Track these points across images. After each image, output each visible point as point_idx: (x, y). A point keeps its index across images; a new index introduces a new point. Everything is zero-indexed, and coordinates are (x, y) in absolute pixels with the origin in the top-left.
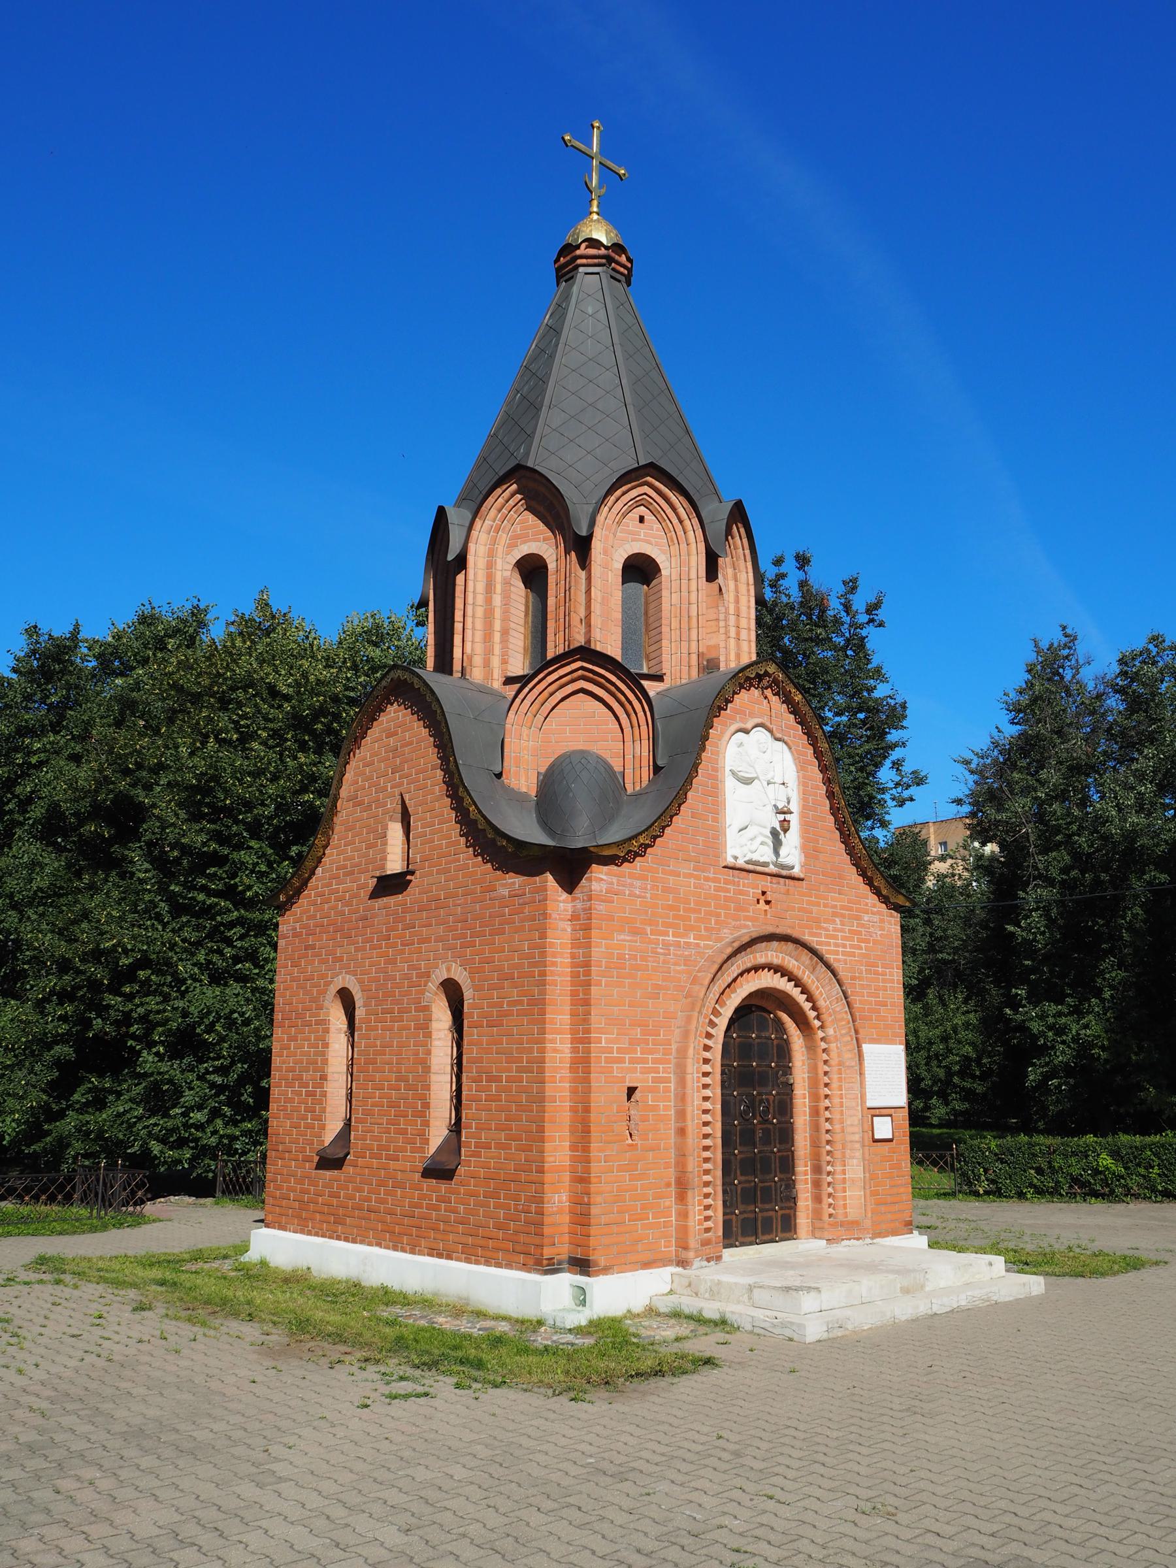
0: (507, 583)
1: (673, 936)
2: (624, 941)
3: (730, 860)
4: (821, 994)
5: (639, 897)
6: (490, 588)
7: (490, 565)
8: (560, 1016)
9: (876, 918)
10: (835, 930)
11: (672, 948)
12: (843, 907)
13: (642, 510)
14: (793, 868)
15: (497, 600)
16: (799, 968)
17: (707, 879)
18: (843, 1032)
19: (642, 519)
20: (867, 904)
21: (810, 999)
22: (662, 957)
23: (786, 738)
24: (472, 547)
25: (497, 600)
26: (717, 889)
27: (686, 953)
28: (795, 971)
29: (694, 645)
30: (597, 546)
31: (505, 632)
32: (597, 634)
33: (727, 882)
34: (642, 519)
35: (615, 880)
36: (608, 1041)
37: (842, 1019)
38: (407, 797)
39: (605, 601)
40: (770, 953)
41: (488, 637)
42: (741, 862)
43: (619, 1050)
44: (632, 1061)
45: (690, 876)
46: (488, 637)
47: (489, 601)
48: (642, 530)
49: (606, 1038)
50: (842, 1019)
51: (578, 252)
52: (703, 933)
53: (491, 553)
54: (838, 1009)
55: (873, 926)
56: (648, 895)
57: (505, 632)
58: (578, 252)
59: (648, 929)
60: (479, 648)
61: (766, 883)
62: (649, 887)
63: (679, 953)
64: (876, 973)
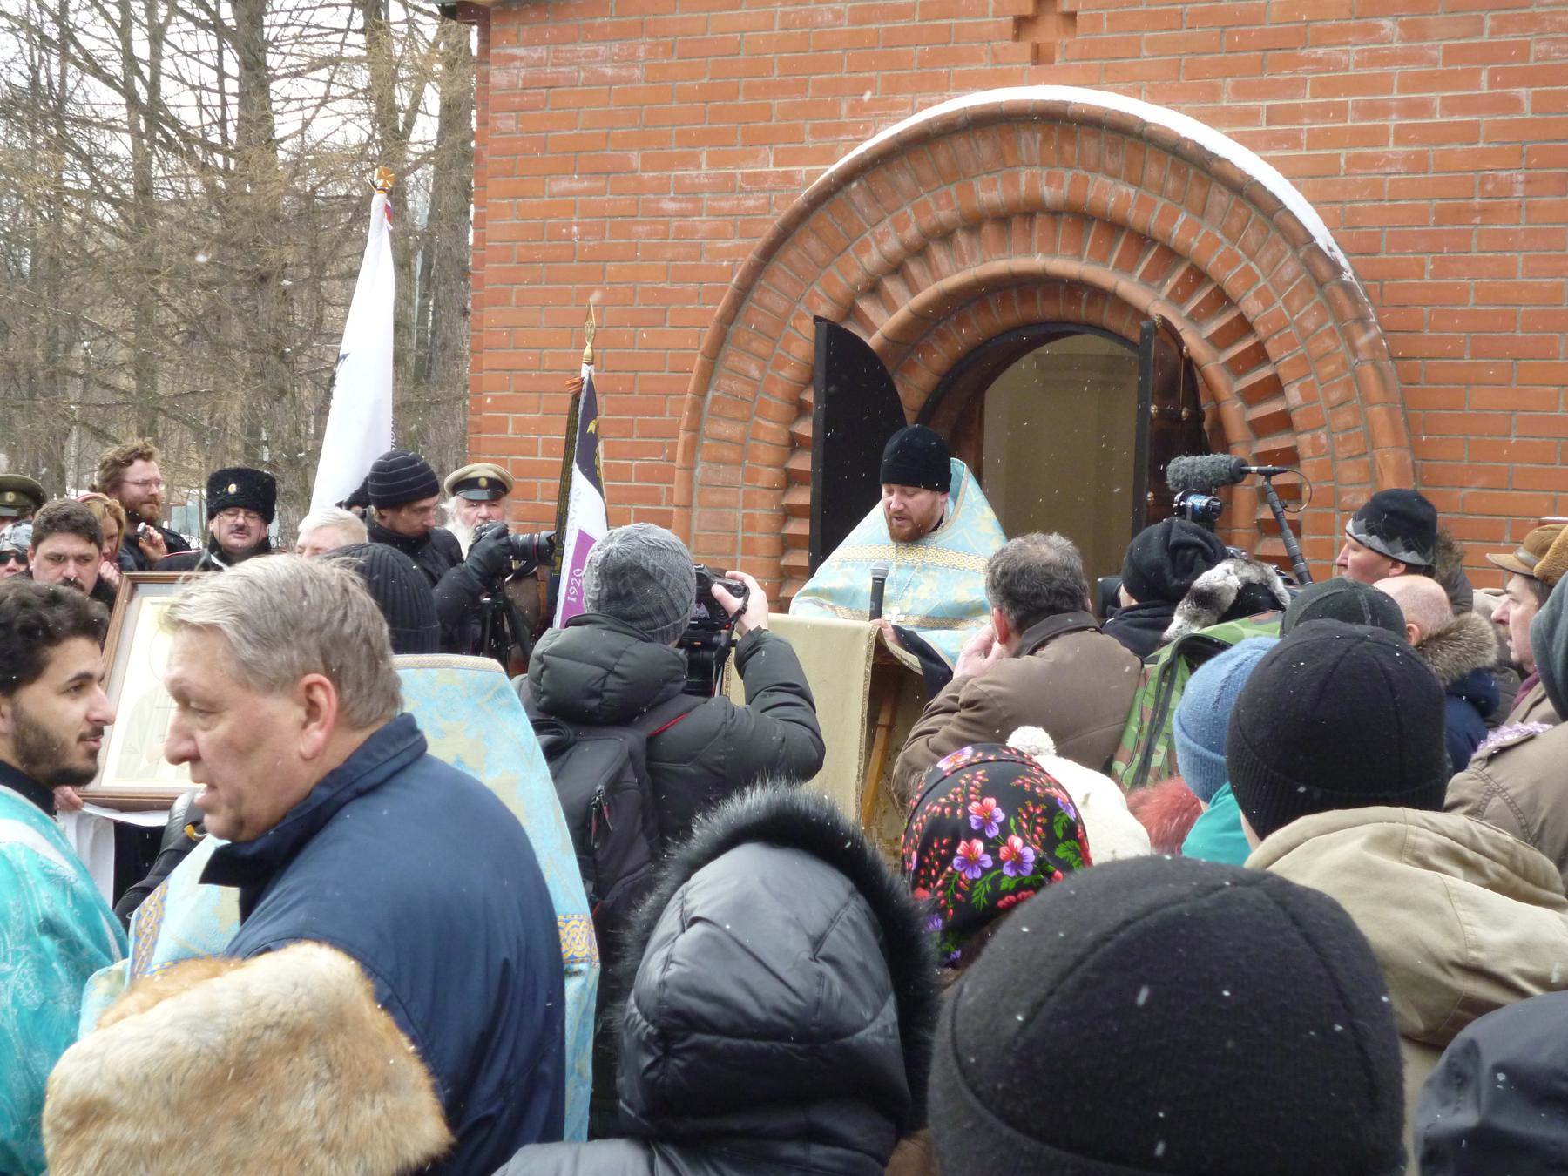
1: (711, 164)
4: (1249, 277)
11: (707, 195)
18: (1335, 396)
22: (675, 222)
27: (750, 203)
28: (1132, 215)
36: (522, 426)
37: (1326, 356)
49: (517, 421)
52: (810, 142)
54: (1309, 324)
56: (637, 72)
62: (641, 52)
63: (726, 205)
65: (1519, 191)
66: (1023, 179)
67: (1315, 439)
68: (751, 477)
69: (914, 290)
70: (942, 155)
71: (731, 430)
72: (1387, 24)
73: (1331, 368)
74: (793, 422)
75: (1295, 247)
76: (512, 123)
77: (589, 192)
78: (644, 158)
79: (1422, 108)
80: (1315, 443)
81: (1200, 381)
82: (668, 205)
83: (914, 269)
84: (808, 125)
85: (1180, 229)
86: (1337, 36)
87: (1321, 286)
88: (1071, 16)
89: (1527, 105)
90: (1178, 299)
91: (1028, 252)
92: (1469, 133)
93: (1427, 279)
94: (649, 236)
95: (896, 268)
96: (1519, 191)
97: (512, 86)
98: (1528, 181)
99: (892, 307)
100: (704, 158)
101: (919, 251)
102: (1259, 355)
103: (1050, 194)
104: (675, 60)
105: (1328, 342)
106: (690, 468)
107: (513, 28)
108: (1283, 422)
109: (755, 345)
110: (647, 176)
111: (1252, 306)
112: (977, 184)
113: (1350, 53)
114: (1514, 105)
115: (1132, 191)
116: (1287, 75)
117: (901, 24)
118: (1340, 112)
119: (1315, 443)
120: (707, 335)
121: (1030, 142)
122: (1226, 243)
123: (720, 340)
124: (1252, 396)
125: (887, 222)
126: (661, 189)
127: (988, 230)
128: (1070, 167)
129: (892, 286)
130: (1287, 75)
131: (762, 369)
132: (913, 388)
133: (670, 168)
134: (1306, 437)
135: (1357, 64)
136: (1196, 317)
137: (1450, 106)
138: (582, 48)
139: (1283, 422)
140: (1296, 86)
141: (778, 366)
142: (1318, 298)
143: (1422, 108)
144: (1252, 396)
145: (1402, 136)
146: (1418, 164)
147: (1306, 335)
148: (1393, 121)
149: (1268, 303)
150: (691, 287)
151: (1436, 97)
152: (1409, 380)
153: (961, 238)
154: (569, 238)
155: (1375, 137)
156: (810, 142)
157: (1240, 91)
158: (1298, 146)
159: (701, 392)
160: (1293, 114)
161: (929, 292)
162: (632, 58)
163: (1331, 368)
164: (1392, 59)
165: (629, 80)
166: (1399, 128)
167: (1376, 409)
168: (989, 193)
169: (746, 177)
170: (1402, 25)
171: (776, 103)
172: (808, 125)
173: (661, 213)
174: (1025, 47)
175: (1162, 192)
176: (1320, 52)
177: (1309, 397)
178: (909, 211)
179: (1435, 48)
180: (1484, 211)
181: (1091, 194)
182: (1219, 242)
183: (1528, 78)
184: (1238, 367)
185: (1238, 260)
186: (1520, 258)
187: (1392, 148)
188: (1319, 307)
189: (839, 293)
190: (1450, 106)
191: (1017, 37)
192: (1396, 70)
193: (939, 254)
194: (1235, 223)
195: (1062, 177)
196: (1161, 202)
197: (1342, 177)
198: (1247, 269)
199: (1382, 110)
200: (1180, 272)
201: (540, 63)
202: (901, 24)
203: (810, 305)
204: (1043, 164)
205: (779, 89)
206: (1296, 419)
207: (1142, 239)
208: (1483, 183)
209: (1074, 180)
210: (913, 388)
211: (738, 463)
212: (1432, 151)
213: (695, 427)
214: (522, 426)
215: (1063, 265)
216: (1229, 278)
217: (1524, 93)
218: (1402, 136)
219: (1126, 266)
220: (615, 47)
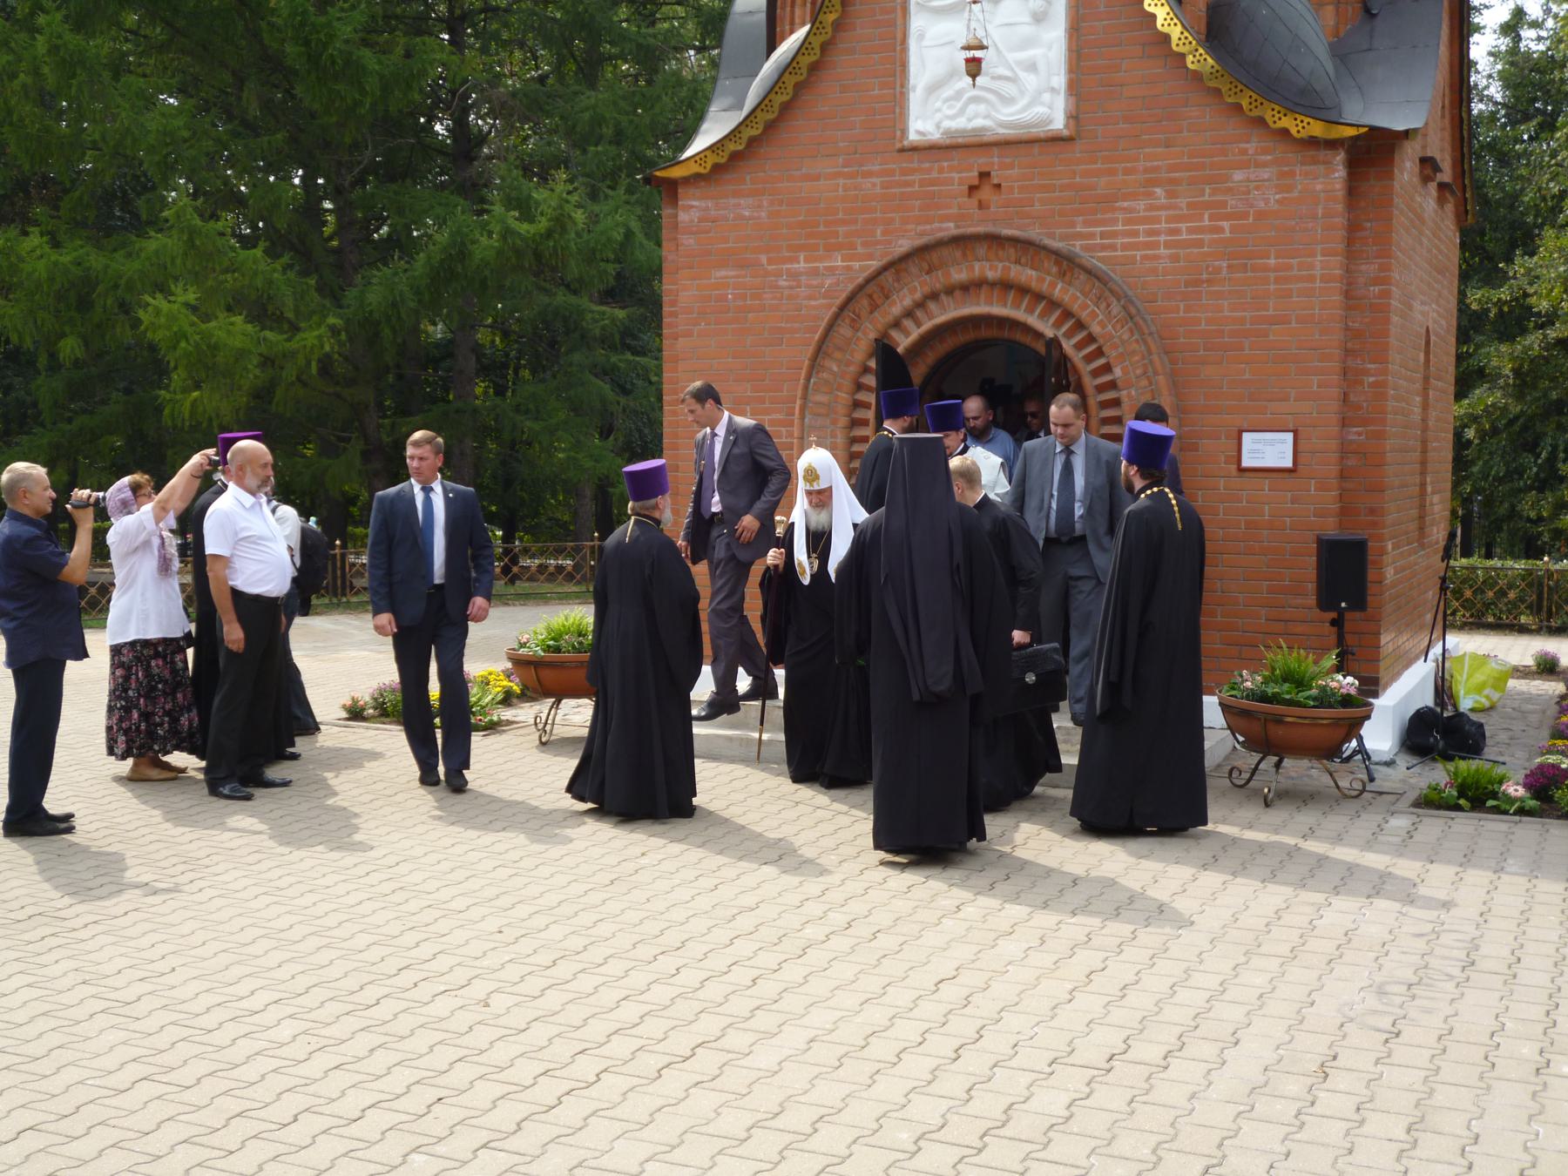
1: (806, 260)
3: (913, 136)
4: (1094, 315)
5: (750, 218)
9: (1265, 174)
10: (1151, 208)
12: (1172, 169)
17: (869, 174)
18: (1138, 372)
20: (1244, 152)
26: (885, 186)
28: (1034, 285)
33: (904, 172)
37: (1134, 352)
40: (977, 266)
42: (935, 136)
52: (860, 250)
54: (1125, 337)
55: (1257, 188)
56: (763, 214)
59: (764, 259)
61: (980, 161)
62: (765, 203)
63: (815, 282)
64: (1266, 269)
65: (1224, 271)
66: (977, 269)
67: (1129, 393)
68: (834, 422)
69: (919, 324)
70: (935, 256)
71: (819, 398)
72: (1158, 191)
73: (1136, 358)
74: (854, 394)
75: (1119, 300)
76: (692, 241)
77: (737, 277)
79: (1176, 232)
81: (1069, 365)
82: (783, 283)
83: (919, 314)
85: (1058, 291)
86: (1133, 196)
87: (1132, 318)
88: (998, 186)
89: (1227, 230)
90: (1057, 325)
91: (978, 304)
92: (1200, 243)
93: (1181, 314)
94: (772, 299)
95: (909, 314)
96: (1224, 271)
97: (692, 221)
98: (1229, 267)
99: (907, 333)
100: (802, 258)
101: (920, 305)
102: (1099, 353)
103: (991, 275)
104: (784, 207)
105: (1135, 346)
106: (802, 418)
107: (691, 191)
108: (1112, 385)
109: (838, 355)
110: (770, 268)
111: (1096, 329)
112: (952, 270)
113: (1141, 205)
114: (1221, 230)
115: (1034, 273)
117: (909, 189)
118: (1135, 234)
119: (1129, 395)
120: (811, 349)
121: (981, 250)
122: (1082, 298)
123: (819, 350)
124: (1096, 373)
125: (905, 290)
126: (779, 274)
127: (958, 293)
128: (1001, 261)
129: (908, 323)
131: (839, 366)
132: (918, 373)
133: (784, 263)
134: (1124, 393)
135: (1145, 210)
136: (1069, 335)
137: (1191, 231)
138: (732, 201)
139: (1112, 385)
140: (1115, 221)
141: (848, 364)
142: (1130, 324)
143: (1176, 232)
144: (1096, 373)
145: (1167, 245)
146: (1175, 258)
147: (1123, 342)
148: (1162, 238)
149: (1103, 327)
150: (796, 325)
151: (1183, 226)
152: (1173, 362)
153: (943, 297)
154: (726, 300)
155: (1155, 245)
156: (860, 250)
157: (1087, 224)
158: (1116, 250)
159: (808, 378)
160: (1114, 235)
161: (927, 325)
163: (1136, 358)
165: (759, 218)
166: (1165, 242)
167: (1161, 377)
168: (959, 275)
169: (825, 268)
170: (1166, 191)
171: (841, 230)
172: (859, 241)
173: (778, 287)
174: (974, 201)
175: (1049, 274)
176: (1126, 204)
177: (1124, 370)
178: (916, 284)
179: (1182, 202)
180: (1209, 281)
181: (1012, 274)
182: (1078, 298)
183: (1227, 217)
184: (1089, 359)
185: (1088, 306)
186: (1226, 303)
187: (1162, 251)
188: (1131, 331)
189: (880, 326)
190: (1191, 231)
191: (970, 196)
192: (1163, 213)
193: (932, 306)
194: (1087, 288)
195: (997, 268)
196: (1049, 278)
197: (1138, 265)
198: (1093, 311)
199: (1157, 233)
200: (1057, 313)
201: (707, 208)
202: (909, 189)
203: (865, 333)
204: (987, 260)
205: (844, 222)
206: (1119, 383)
207: (1038, 297)
208: (1207, 267)
209: (1004, 267)
210: (918, 373)
211: (827, 415)
212: (1181, 251)
213: (805, 397)
215: (997, 310)
216: (1084, 315)
217: (1226, 224)
218: (1167, 245)
219: (1030, 310)
220: (750, 201)
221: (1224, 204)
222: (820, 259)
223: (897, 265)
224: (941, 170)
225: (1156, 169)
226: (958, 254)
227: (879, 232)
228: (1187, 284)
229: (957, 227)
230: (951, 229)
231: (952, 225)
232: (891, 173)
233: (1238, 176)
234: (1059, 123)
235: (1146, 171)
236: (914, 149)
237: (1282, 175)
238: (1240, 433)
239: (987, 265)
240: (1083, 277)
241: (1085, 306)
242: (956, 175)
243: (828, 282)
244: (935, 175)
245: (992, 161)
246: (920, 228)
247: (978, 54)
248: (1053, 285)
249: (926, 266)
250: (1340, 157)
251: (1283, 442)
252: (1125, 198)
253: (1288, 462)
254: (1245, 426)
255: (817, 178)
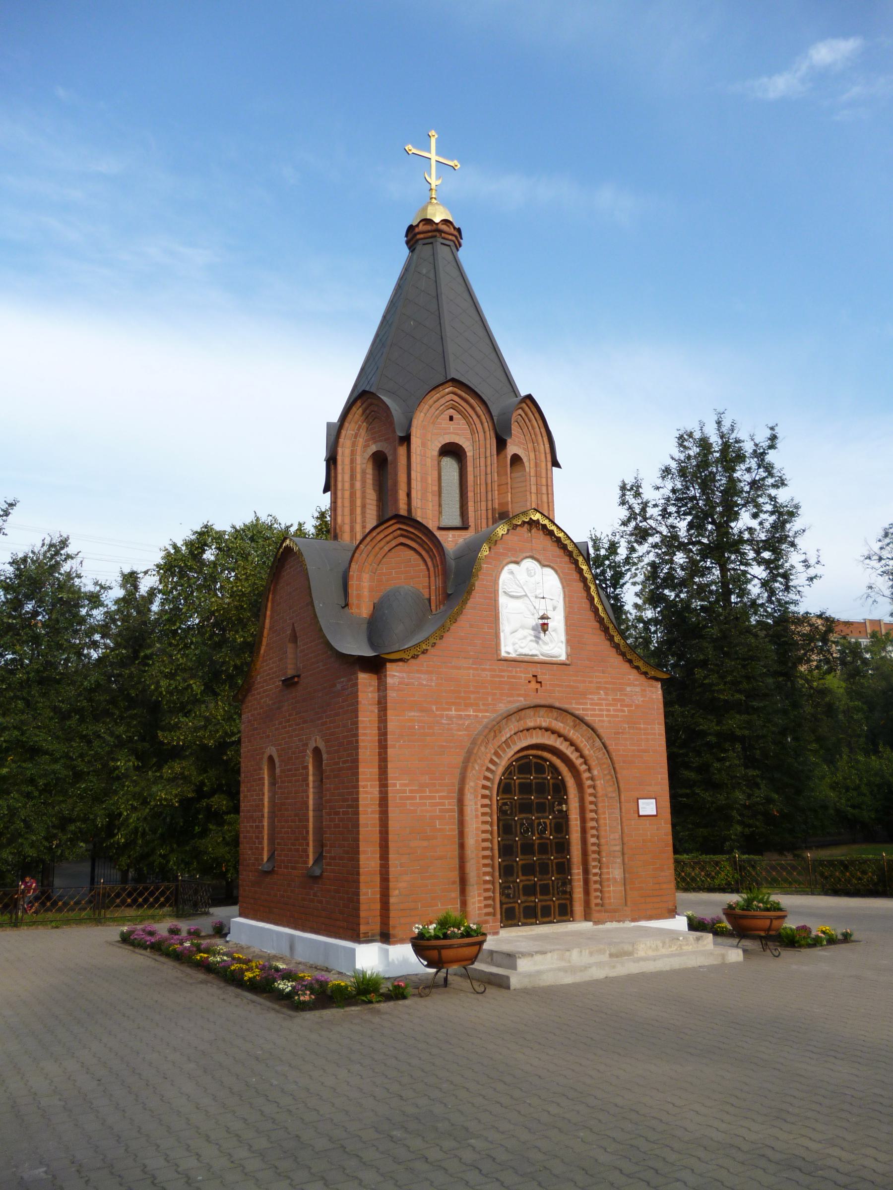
0: (364, 472)
1: (456, 710)
2: (414, 716)
3: (503, 654)
5: (426, 685)
6: (353, 478)
7: (352, 461)
8: (368, 772)
9: (638, 689)
10: (600, 699)
12: (606, 683)
13: (451, 412)
14: (560, 656)
15: (358, 485)
16: (564, 728)
17: (484, 670)
19: (451, 418)
20: (629, 679)
21: (577, 749)
23: (552, 564)
24: (340, 450)
25: (358, 485)
26: (493, 676)
28: (562, 731)
29: (490, 503)
30: (415, 441)
31: (364, 506)
32: (416, 502)
34: (451, 418)
35: (405, 675)
36: (401, 785)
37: (604, 764)
38: (296, 625)
39: (424, 479)
40: (538, 719)
41: (352, 511)
42: (513, 655)
43: (411, 791)
44: (421, 798)
45: (470, 668)
46: (352, 511)
47: (352, 486)
48: (452, 426)
49: (400, 784)
50: (604, 764)
51: (417, 230)
52: (482, 707)
53: (353, 453)
55: (635, 695)
56: (433, 684)
57: (364, 506)
58: (417, 230)
60: (347, 520)
61: (533, 670)
62: (434, 678)
63: (460, 722)
64: (640, 729)
73: (605, 766)
78: (437, 708)
80: (601, 783)
84: (481, 703)
85: (572, 734)
92: (617, 716)
103: (544, 725)
113: (596, 697)
114: (623, 711)
116: (584, 701)
119: (601, 783)
121: (542, 711)
126: (442, 716)
128: (548, 718)
130: (584, 701)
138: (417, 675)
140: (586, 704)
145: (607, 716)
146: (609, 722)
148: (605, 713)
151: (611, 708)
154: (415, 729)
157: (577, 703)
162: (431, 680)
164: (603, 699)
165: (430, 686)
168: (531, 724)
171: (472, 696)
173: (442, 724)
176: (590, 696)
177: (598, 771)
179: (610, 698)
180: (622, 733)
183: (627, 706)
187: (605, 719)
188: (604, 754)
192: (604, 702)
201: (403, 677)
205: (473, 692)
214: (401, 785)
217: (626, 709)
220: (426, 676)
221: (624, 700)
222: (444, 709)
223: (508, 716)
224: (516, 672)
225: (600, 682)
226: (532, 713)
227: (490, 700)
228: (616, 733)
229: (525, 700)
230: (522, 701)
231: (522, 699)
232: (494, 670)
233: (628, 689)
234: (563, 658)
235: (597, 682)
236: (506, 660)
237: (642, 690)
238: (638, 799)
239: (542, 719)
240: (585, 727)
241: (582, 742)
242: (523, 675)
243: (467, 723)
244: (514, 674)
245: (538, 670)
246: (509, 699)
247: (546, 621)
248: (569, 731)
249: (518, 718)
250: (659, 685)
251: (652, 803)
252: (591, 693)
253: (654, 813)
254: (638, 797)
255: (459, 668)
